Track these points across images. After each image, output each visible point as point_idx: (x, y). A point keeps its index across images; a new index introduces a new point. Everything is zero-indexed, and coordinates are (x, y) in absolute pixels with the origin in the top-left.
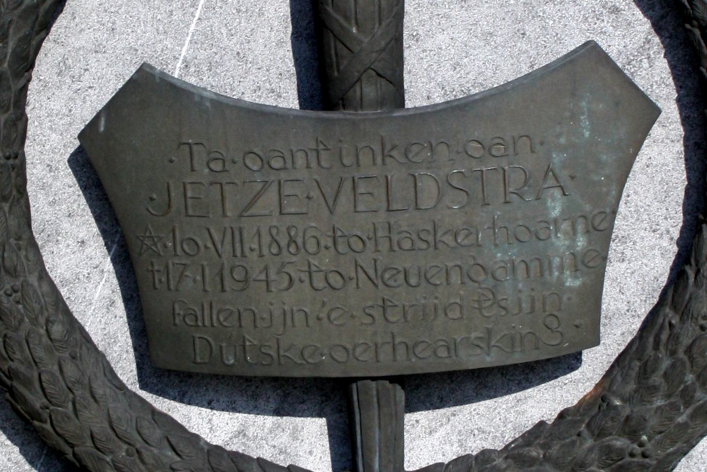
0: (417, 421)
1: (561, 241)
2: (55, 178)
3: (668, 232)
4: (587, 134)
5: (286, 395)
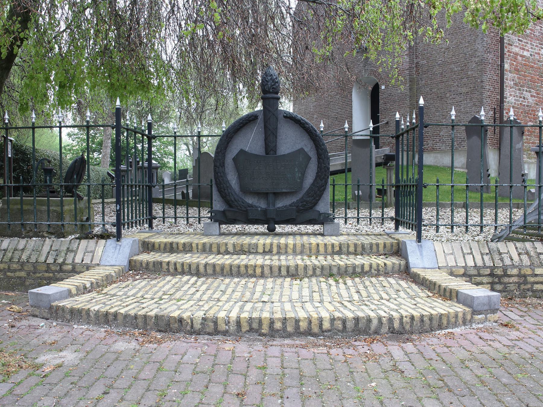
1: (297, 175)
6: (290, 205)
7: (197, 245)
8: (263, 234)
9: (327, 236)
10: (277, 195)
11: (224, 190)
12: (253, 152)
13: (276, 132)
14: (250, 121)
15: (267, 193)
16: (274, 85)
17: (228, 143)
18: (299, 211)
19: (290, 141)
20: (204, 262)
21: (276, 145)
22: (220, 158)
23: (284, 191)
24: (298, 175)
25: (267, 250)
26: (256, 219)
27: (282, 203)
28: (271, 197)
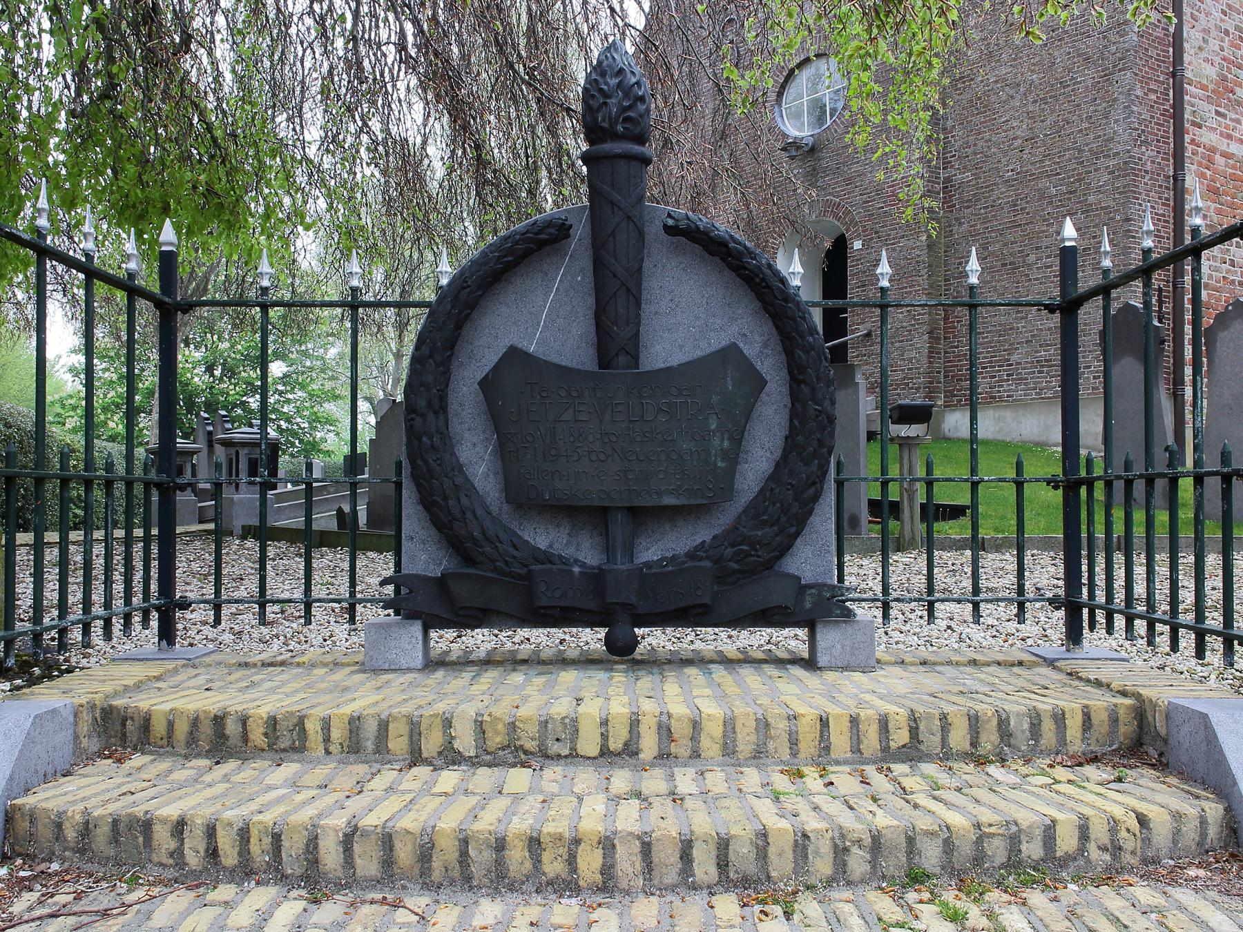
1: (716, 442)
6: (692, 555)
7: (326, 725)
8: (587, 661)
9: (830, 669)
10: (643, 516)
11: (446, 498)
12: (554, 358)
13: (639, 285)
14: (542, 244)
16: (630, 108)
17: (459, 326)
18: (724, 577)
19: (687, 320)
20: (339, 821)
21: (637, 334)
22: (430, 378)
23: (668, 501)
24: (720, 443)
25: (615, 744)
26: (564, 609)
27: (658, 548)
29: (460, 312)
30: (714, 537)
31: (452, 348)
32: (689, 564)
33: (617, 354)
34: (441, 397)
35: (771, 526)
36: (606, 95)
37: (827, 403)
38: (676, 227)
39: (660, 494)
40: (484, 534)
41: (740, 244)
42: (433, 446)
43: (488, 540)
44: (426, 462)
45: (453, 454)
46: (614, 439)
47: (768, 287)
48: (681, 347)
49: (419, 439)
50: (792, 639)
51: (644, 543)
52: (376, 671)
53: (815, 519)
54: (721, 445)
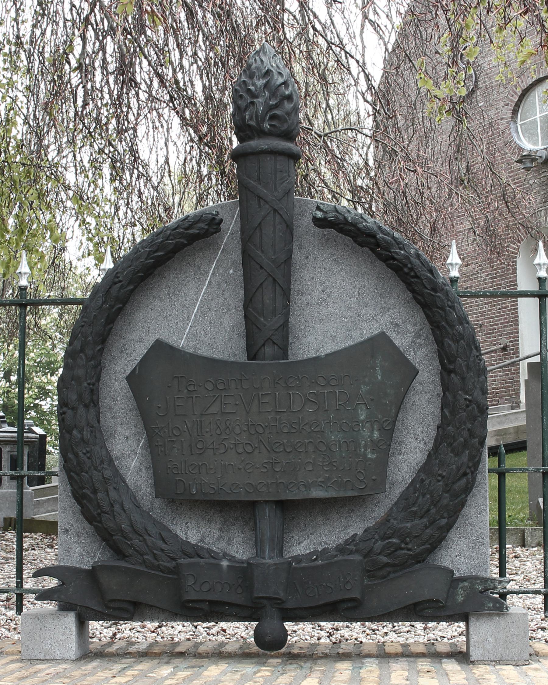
0: (293, 537)
1: (366, 433)
2: (115, 405)
3: (423, 440)
4: (380, 378)
5: (225, 521)
6: (341, 549)
8: (243, 655)
9: (483, 662)
10: (292, 510)
11: (95, 492)
12: (205, 352)
13: (288, 277)
14: (193, 239)
15: (253, 504)
16: (276, 106)
18: (374, 571)
22: (80, 372)
23: (317, 493)
24: (369, 434)
26: (212, 603)
28: (268, 519)
29: (112, 307)
30: (365, 531)
31: (104, 341)
32: (340, 558)
33: (264, 345)
34: (92, 391)
35: (421, 517)
36: (253, 95)
37: (477, 393)
38: (324, 219)
39: (308, 487)
40: (132, 526)
41: (388, 234)
42: (82, 439)
43: (135, 531)
44: (76, 455)
45: (104, 446)
46: (261, 430)
47: (416, 276)
48: (333, 338)
49: (70, 432)
50: (448, 632)
51: (296, 537)
52: (32, 661)
53: (469, 511)
54: (371, 436)
